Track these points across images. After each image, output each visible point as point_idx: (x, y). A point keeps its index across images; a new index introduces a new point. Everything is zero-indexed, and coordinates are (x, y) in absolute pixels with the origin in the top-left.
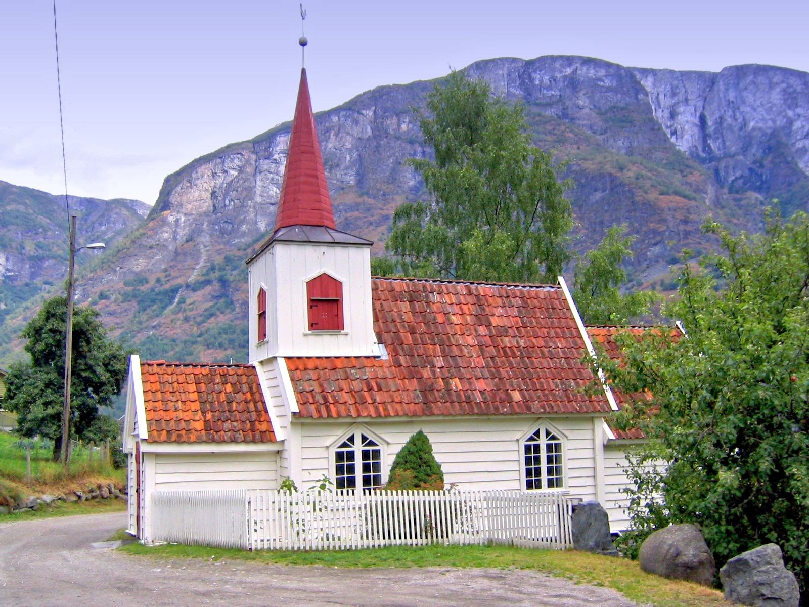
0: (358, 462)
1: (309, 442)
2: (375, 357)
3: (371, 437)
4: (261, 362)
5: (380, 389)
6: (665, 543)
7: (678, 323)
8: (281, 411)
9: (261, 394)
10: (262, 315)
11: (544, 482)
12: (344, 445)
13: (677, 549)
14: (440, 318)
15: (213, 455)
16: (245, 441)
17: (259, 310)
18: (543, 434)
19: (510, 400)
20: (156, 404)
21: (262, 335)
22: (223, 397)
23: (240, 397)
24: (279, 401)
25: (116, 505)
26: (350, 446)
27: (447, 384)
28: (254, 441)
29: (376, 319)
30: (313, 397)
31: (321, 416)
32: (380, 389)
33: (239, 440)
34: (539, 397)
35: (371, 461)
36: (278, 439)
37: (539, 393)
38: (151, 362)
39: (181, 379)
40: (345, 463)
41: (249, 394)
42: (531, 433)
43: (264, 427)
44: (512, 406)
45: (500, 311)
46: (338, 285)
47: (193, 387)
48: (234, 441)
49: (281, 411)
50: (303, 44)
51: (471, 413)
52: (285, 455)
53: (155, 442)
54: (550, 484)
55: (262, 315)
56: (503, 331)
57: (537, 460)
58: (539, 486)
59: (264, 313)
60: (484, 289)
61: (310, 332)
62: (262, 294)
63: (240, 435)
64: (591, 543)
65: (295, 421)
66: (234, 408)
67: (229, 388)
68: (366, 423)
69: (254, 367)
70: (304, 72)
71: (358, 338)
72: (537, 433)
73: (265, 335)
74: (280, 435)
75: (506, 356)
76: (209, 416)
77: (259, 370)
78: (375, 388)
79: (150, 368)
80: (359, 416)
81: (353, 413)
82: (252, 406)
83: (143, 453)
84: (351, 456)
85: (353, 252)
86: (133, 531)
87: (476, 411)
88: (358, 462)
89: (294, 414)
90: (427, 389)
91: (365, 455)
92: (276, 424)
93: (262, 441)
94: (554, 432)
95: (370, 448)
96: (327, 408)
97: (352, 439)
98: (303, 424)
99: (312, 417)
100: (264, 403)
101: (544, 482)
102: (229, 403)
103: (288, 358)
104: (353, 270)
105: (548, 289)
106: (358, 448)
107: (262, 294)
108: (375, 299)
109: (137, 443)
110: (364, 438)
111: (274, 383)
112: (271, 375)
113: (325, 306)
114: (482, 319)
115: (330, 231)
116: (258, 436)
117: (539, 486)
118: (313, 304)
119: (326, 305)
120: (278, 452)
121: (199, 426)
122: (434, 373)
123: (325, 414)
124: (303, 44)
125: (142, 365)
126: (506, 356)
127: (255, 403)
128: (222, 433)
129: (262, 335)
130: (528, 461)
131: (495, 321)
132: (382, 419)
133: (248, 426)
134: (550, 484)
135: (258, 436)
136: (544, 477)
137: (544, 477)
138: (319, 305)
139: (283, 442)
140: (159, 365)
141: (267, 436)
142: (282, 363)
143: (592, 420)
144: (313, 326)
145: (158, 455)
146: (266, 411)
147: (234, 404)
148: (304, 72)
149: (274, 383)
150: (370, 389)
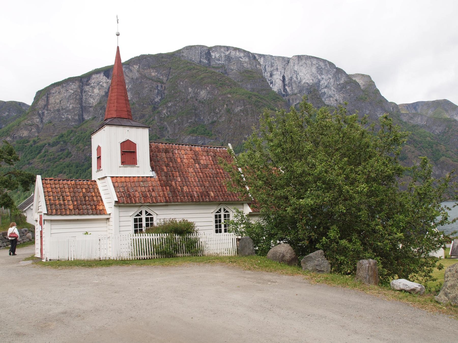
1: (122, 214)
2: (151, 177)
3: (149, 212)
4: (99, 179)
5: (153, 191)
6: (278, 252)
8: (109, 200)
9: (99, 193)
10: (99, 158)
11: (223, 230)
12: (138, 215)
13: (283, 254)
14: (179, 160)
15: (78, 220)
16: (93, 214)
17: (97, 155)
18: (222, 210)
19: (209, 195)
20: (50, 198)
21: (99, 167)
23: (89, 194)
24: (108, 196)
25: (30, 244)
27: (182, 189)
28: (97, 214)
29: (151, 161)
30: (124, 194)
31: (132, 203)
32: (153, 191)
34: (221, 194)
35: (149, 222)
37: (221, 193)
39: (61, 186)
40: (138, 223)
41: (93, 193)
42: (218, 210)
43: (101, 208)
44: (209, 199)
45: (204, 158)
46: (134, 145)
48: (88, 214)
49: (109, 200)
50: (118, 35)
51: (193, 201)
52: (110, 220)
53: (51, 215)
54: (225, 231)
55: (99, 158)
56: (206, 166)
57: (220, 221)
58: (221, 232)
59: (100, 157)
60: (197, 148)
62: (99, 149)
63: (91, 211)
64: (247, 254)
65: (116, 205)
67: (84, 190)
68: (147, 206)
69: (95, 181)
70: (118, 48)
71: (143, 168)
72: (220, 210)
75: (207, 177)
76: (75, 203)
77: (98, 182)
78: (152, 191)
79: (46, 181)
80: (145, 203)
81: (143, 201)
82: (95, 198)
83: (44, 220)
84: (141, 220)
85: (140, 130)
86: (39, 255)
87: (195, 200)
89: (116, 202)
90: (174, 191)
91: (147, 219)
93: (101, 214)
94: (227, 209)
95: (149, 216)
96: (130, 199)
97: (141, 213)
98: (119, 206)
99: (123, 203)
100: (101, 197)
101: (223, 230)
102: (85, 197)
103: (112, 177)
104: (141, 137)
105: (224, 149)
106: (144, 216)
107: (99, 149)
108: (151, 151)
109: (41, 216)
110: (146, 212)
111: (105, 188)
112: (104, 184)
113: (128, 153)
114: (197, 161)
115: (130, 121)
116: (98, 212)
117: (221, 232)
118: (123, 153)
119: (129, 154)
120: (108, 219)
121: (71, 207)
122: (176, 184)
123: (129, 202)
124: (118, 35)
125: (42, 180)
126: (207, 177)
127: (97, 197)
129: (99, 167)
130: (216, 222)
131: (202, 162)
132: (155, 204)
133: (94, 207)
134: (225, 231)
135: (98, 212)
136: (223, 228)
137: (223, 228)
138: (126, 154)
139: (110, 214)
140: (50, 180)
141: (102, 212)
142: (109, 179)
143: (243, 204)
144: (123, 163)
145: (51, 221)
146: (102, 200)
147: (87, 197)
148: (118, 48)
149: (105, 188)
150: (149, 191)
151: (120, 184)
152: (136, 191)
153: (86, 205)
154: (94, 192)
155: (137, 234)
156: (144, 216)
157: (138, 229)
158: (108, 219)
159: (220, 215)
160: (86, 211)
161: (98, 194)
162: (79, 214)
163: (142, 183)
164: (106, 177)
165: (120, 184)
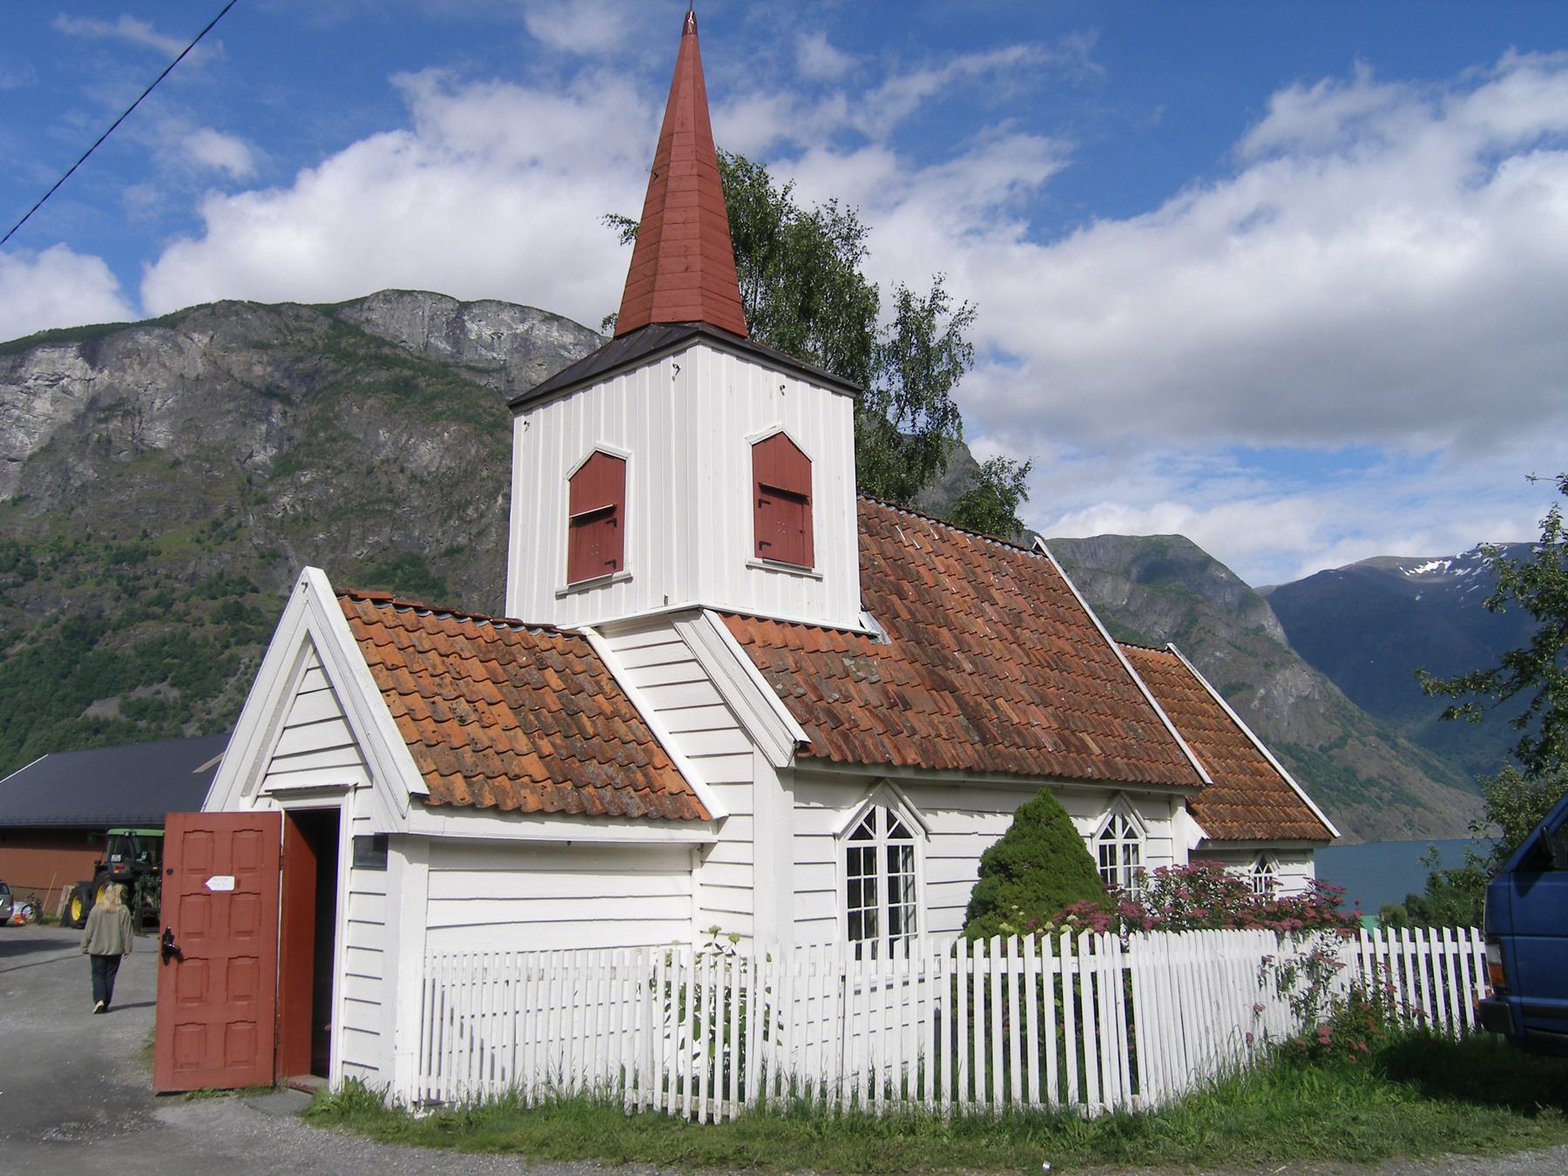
0: (882, 875)
2: (872, 637)
4: (597, 628)
7: (1170, 645)
12: (861, 834)
14: (927, 577)
22: (552, 702)
26: (871, 838)
33: (636, 813)
36: (716, 814)
38: (360, 594)
41: (600, 698)
47: (476, 668)
61: (760, 561)
66: (591, 731)
69: (583, 638)
73: (616, 563)
74: (715, 803)
88: (882, 875)
89: (801, 747)
92: (696, 775)
96: (845, 736)
106: (881, 840)
119: (783, 502)
128: (590, 789)
139: (720, 822)
144: (761, 546)
151: (781, 650)
152: (848, 699)
153: (559, 764)
154: (601, 691)
155: (866, 944)
156: (881, 840)
157: (863, 908)
158: (703, 848)
159: (1113, 847)
160: (608, 793)
161: (624, 709)
162: (586, 816)
163: (847, 662)
164: (696, 611)
165: (781, 650)
